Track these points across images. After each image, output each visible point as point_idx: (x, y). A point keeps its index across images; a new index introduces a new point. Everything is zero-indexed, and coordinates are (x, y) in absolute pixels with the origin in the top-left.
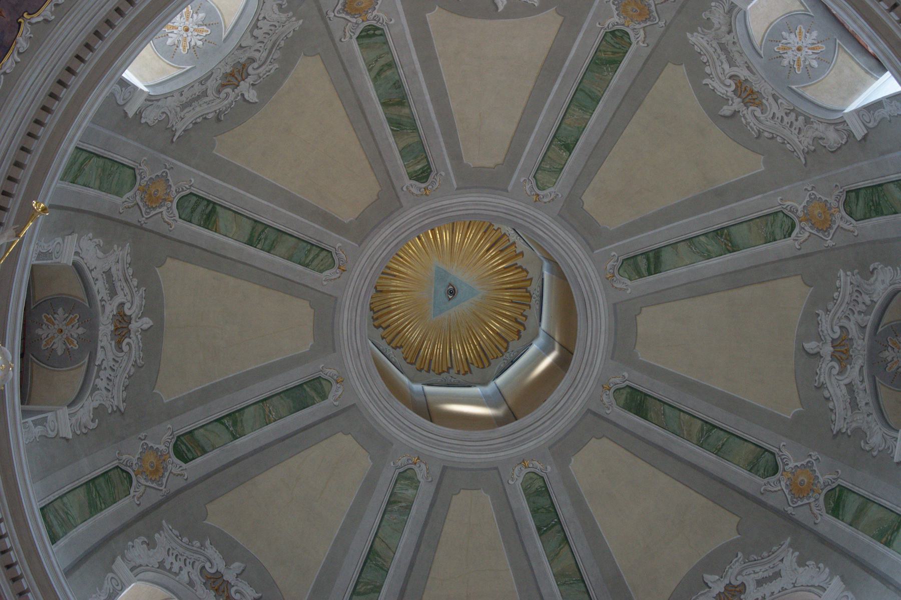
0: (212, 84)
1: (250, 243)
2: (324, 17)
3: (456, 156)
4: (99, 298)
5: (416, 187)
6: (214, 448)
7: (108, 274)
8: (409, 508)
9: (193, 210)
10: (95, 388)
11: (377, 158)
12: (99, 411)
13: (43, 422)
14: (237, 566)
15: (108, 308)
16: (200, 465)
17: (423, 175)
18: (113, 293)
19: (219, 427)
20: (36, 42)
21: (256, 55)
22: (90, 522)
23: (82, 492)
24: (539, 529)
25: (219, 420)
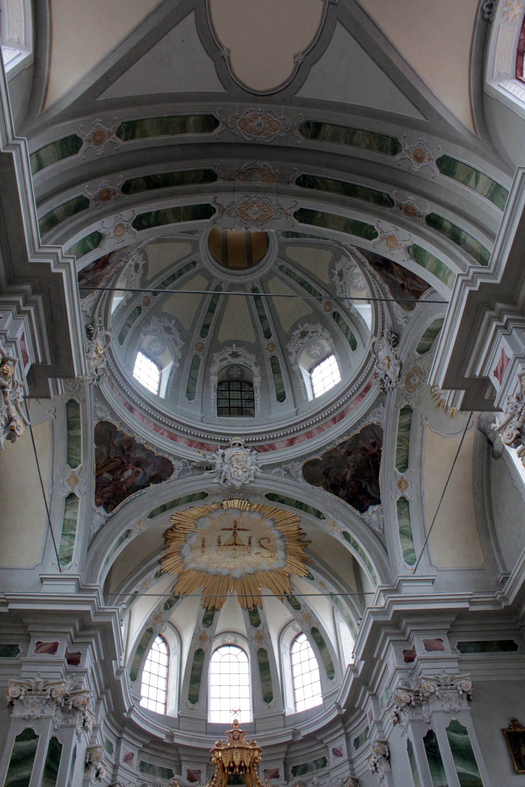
0: (171, 337)
1: (213, 312)
2: (151, 310)
3: (189, 256)
4: (227, 364)
5: (198, 265)
6: (268, 325)
7: (221, 361)
8: (289, 270)
9: (205, 333)
10: (250, 366)
11: (190, 278)
12: (256, 366)
13: (256, 389)
14: (300, 326)
15: (230, 360)
16: (273, 331)
17: (194, 263)
18: (226, 359)
19: (264, 323)
20: (161, 450)
21: (162, 326)
22: (283, 375)
23: (276, 376)
24: (297, 237)
25: (262, 322)
